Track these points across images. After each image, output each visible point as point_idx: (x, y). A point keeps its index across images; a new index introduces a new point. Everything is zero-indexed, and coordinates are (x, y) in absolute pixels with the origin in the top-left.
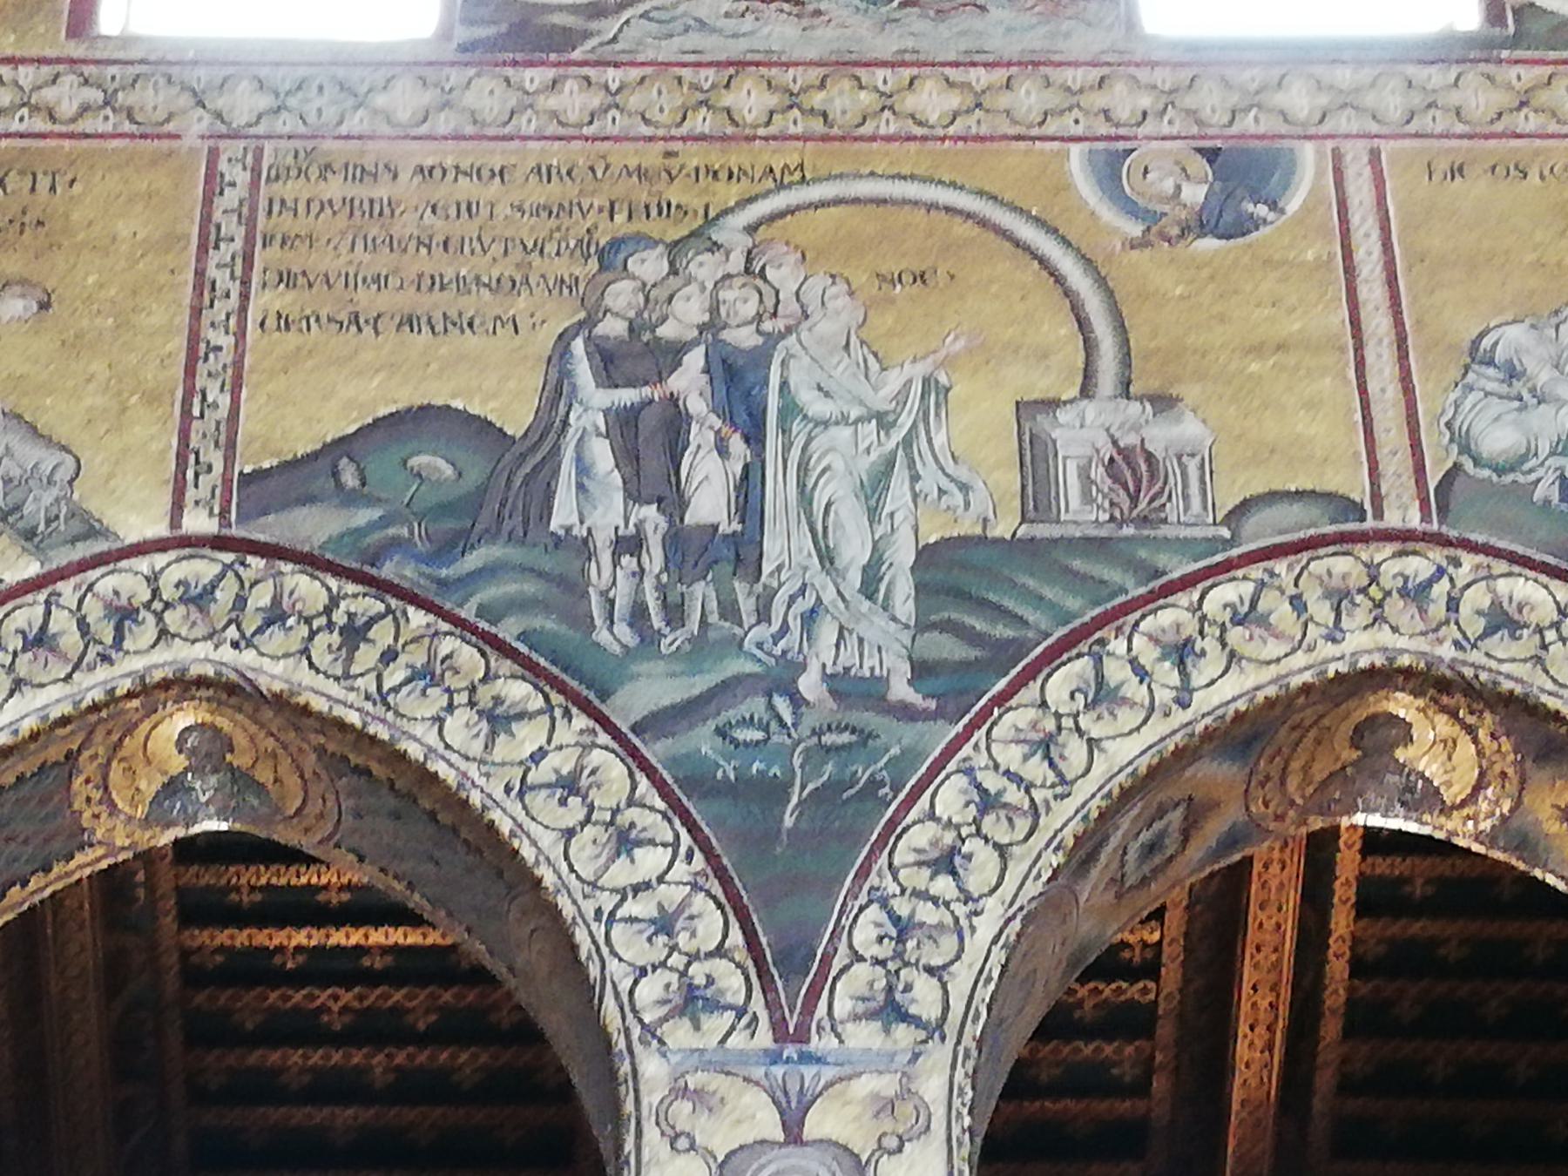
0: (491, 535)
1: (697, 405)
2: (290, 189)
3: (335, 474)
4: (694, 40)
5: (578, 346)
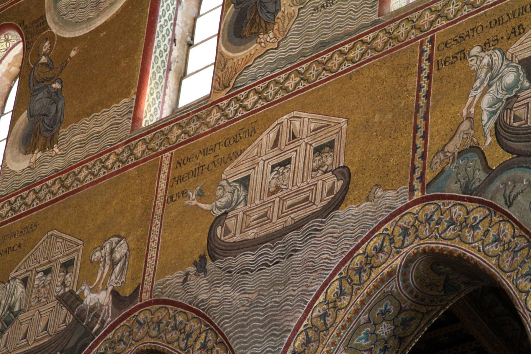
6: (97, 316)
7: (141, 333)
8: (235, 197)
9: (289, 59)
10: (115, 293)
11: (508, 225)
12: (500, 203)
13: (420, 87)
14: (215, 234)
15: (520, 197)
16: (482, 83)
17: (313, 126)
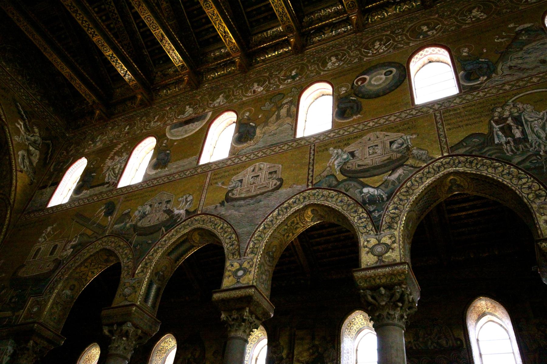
0: (487, 146)
1: (512, 124)
2: (445, 115)
3: (463, 145)
4: (497, 83)
5: (492, 122)
6: (179, 217)
7: (196, 223)
8: (237, 185)
9: (259, 148)
10: (187, 211)
11: (345, 197)
12: (343, 191)
13: (310, 158)
14: (228, 195)
15: (351, 189)
16: (334, 157)
17: (268, 166)
